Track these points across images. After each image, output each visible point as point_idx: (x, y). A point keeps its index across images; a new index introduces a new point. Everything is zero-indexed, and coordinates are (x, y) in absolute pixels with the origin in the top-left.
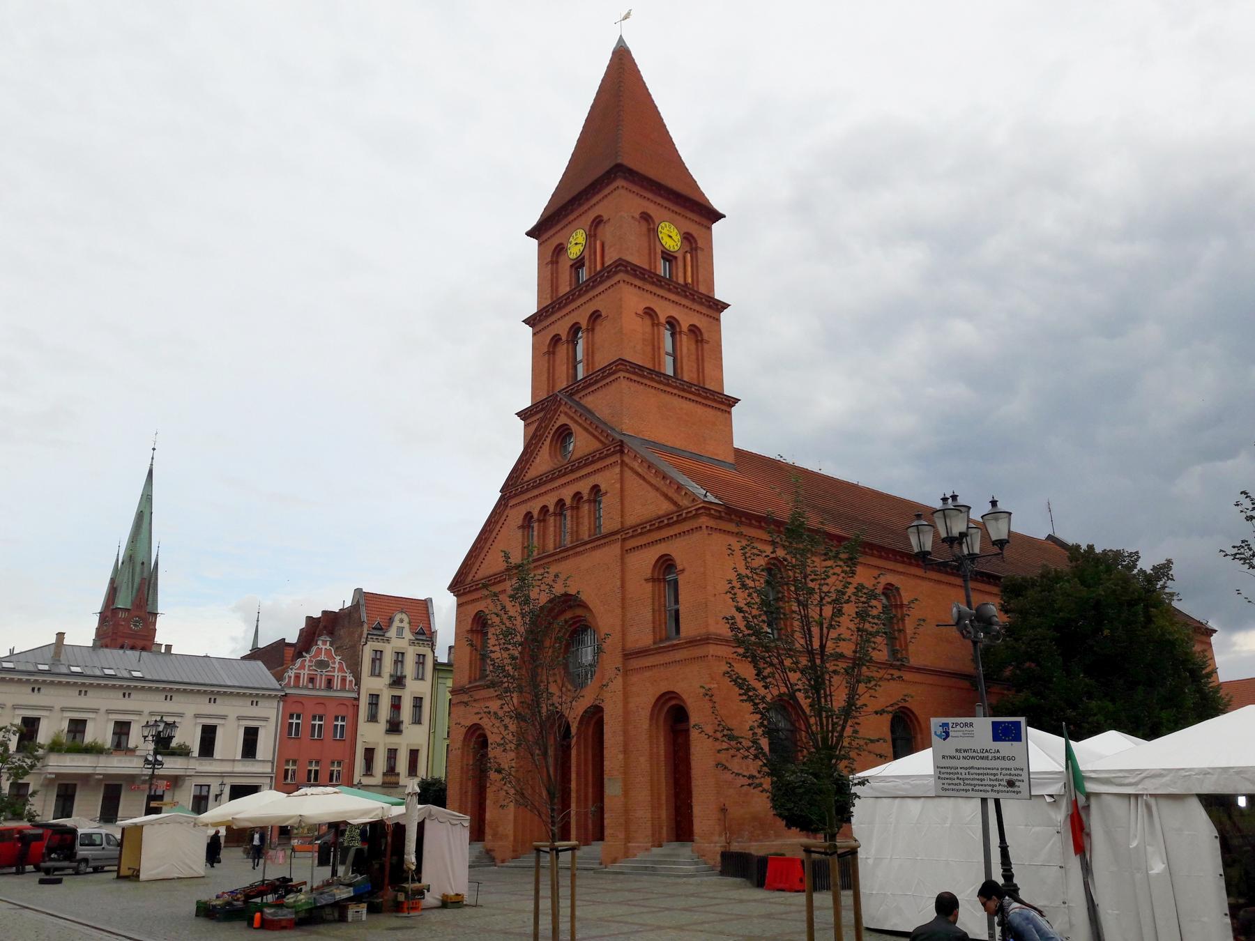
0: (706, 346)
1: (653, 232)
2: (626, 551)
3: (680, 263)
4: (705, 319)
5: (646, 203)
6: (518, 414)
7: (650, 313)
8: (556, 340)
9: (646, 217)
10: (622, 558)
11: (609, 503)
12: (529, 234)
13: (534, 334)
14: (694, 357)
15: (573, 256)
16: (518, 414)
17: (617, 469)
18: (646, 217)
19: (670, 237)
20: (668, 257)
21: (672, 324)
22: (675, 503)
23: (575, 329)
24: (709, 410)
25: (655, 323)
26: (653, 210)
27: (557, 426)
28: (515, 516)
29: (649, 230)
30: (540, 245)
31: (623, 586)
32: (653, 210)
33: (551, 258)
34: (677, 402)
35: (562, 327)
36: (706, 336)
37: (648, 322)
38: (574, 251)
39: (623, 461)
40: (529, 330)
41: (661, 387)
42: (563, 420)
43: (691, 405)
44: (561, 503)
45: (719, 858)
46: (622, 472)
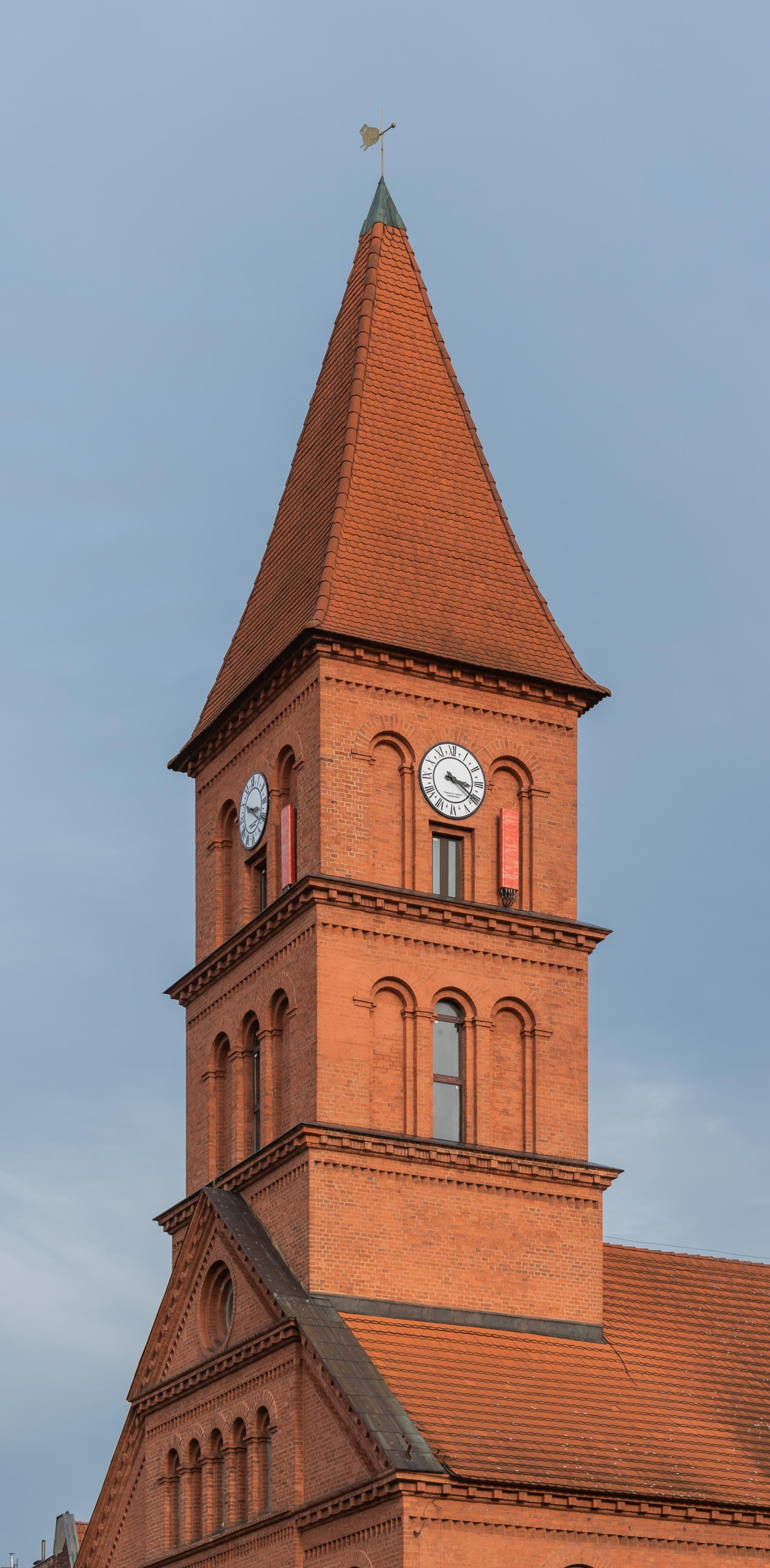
0: (543, 1046)
3: (484, 843)
4: (538, 976)
7: (393, 986)
14: (514, 1076)
18: (391, 739)
20: (449, 831)
21: (455, 1000)
24: (538, 1205)
26: (405, 718)
32: (405, 718)
34: (451, 1200)
36: (542, 1022)
41: (414, 1169)
43: (492, 1203)
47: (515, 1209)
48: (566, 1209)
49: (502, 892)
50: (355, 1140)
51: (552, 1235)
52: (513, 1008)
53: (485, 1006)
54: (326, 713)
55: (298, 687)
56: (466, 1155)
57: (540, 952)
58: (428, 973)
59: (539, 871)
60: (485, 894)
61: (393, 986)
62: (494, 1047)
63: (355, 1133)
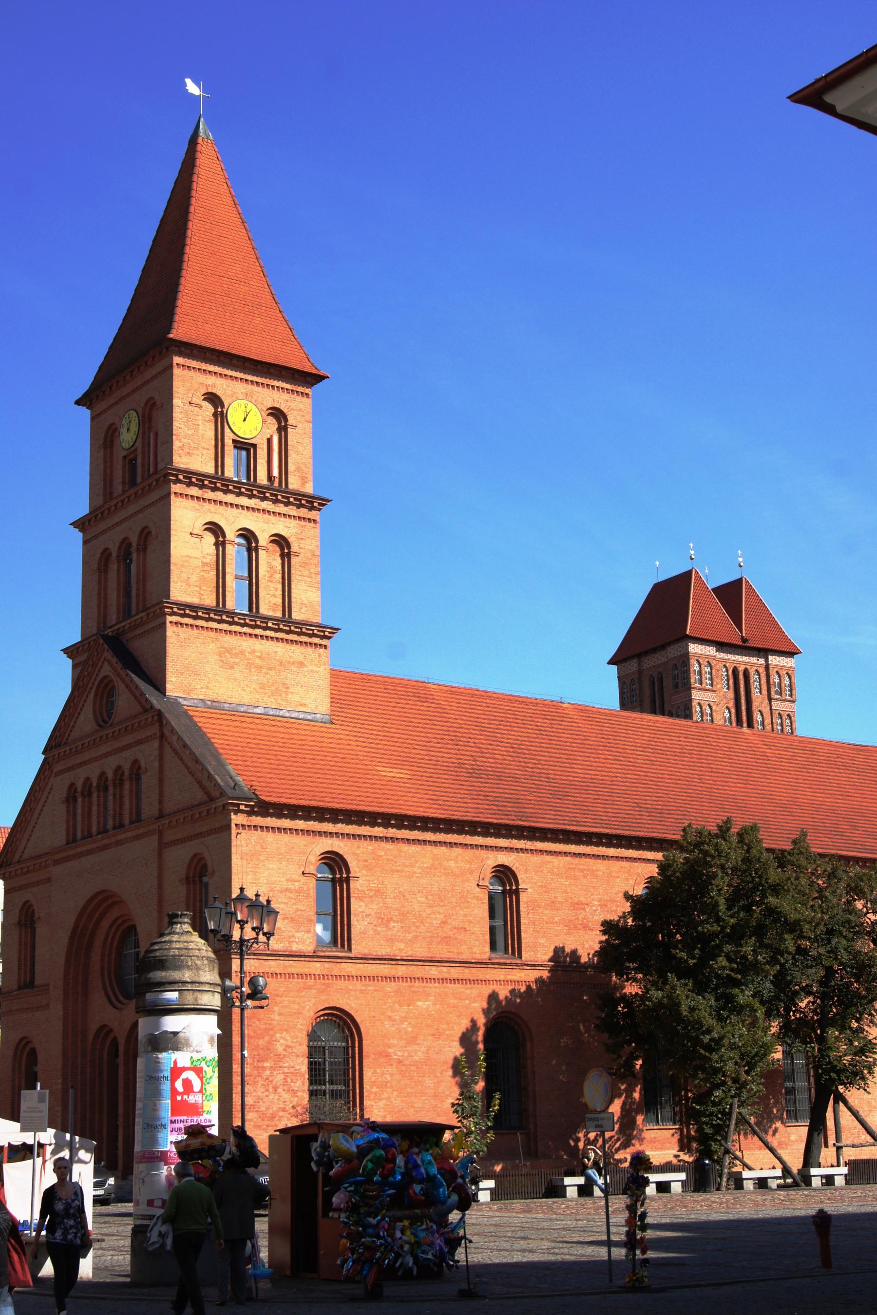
0: (294, 560)
1: (220, 418)
2: (162, 846)
3: (262, 454)
4: (294, 523)
5: (210, 380)
6: (66, 651)
7: (215, 529)
8: (106, 555)
9: (213, 399)
10: (160, 855)
11: (149, 780)
12: (78, 403)
13: (85, 542)
14: (279, 576)
15: (126, 445)
16: (66, 651)
17: (156, 744)
18: (213, 399)
19: (248, 418)
20: (244, 446)
21: (248, 536)
22: (207, 793)
23: (125, 545)
24: (294, 647)
25: (221, 543)
26: (221, 386)
27: (100, 677)
28: (60, 785)
29: (215, 415)
30: (93, 419)
31: (160, 887)
32: (221, 386)
33: (104, 440)
34: (247, 644)
35: (112, 541)
36: (295, 548)
37: (210, 539)
38: (128, 436)
39: (162, 736)
40: (78, 536)
41: (224, 626)
42: (106, 670)
43: (268, 646)
44: (103, 774)
45: (813, 1228)
46: (161, 747)
47: (280, 649)
48: (309, 650)
49: (270, 478)
50: (191, 611)
51: (302, 664)
52: (281, 542)
53: (263, 539)
54: (176, 383)
55: (159, 367)
56: (254, 620)
57: (292, 511)
58: (232, 522)
59: (291, 467)
60: (262, 477)
61: (215, 529)
62: (269, 562)
63: (194, 608)
